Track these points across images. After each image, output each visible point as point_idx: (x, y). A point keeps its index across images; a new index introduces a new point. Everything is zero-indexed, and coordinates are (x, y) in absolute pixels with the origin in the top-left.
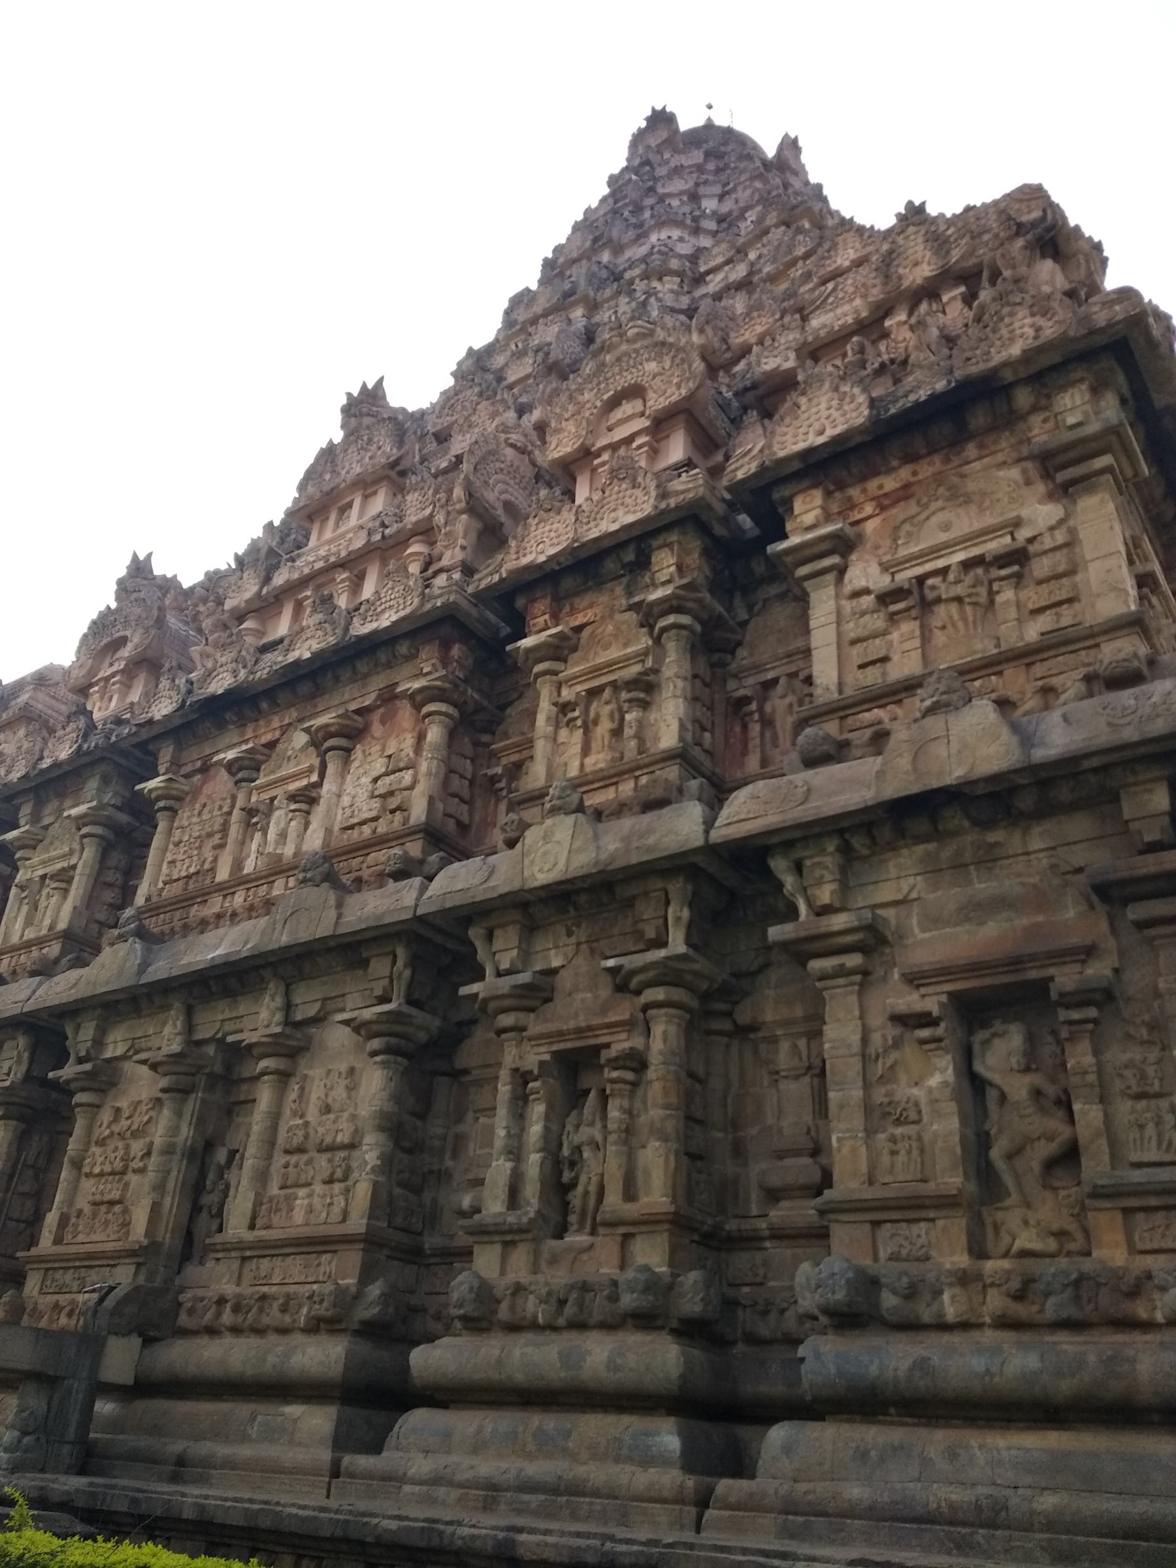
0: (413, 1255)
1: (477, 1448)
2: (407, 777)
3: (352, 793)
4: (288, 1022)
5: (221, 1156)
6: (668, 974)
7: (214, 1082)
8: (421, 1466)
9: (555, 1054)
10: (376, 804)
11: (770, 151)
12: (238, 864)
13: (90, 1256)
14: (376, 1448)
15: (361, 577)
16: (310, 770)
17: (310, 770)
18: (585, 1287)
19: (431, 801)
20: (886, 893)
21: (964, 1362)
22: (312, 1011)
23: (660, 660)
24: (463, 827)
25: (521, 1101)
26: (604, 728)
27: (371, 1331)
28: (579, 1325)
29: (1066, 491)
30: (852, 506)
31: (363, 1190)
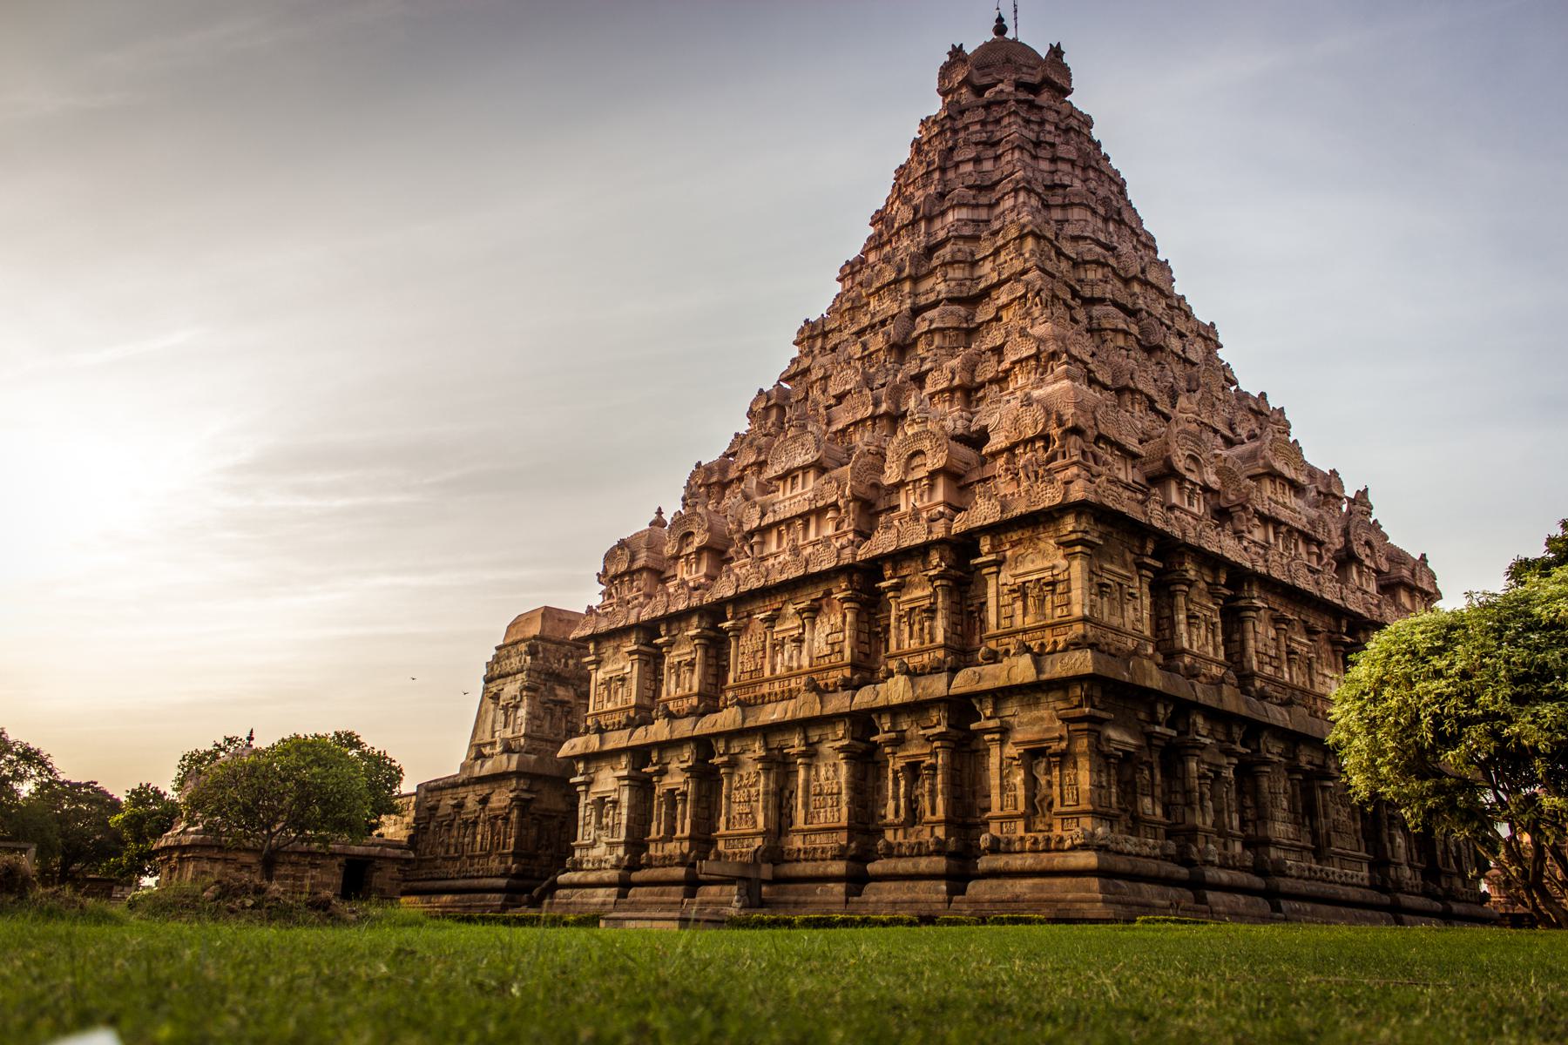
0: (867, 832)
1: (890, 892)
4: (807, 744)
5: (787, 793)
6: (940, 736)
7: (779, 766)
8: (873, 898)
11: (1043, 53)
12: (773, 669)
14: (859, 895)
18: (920, 844)
21: (1016, 862)
22: (816, 739)
24: (867, 656)
27: (852, 859)
28: (919, 855)
31: (845, 810)
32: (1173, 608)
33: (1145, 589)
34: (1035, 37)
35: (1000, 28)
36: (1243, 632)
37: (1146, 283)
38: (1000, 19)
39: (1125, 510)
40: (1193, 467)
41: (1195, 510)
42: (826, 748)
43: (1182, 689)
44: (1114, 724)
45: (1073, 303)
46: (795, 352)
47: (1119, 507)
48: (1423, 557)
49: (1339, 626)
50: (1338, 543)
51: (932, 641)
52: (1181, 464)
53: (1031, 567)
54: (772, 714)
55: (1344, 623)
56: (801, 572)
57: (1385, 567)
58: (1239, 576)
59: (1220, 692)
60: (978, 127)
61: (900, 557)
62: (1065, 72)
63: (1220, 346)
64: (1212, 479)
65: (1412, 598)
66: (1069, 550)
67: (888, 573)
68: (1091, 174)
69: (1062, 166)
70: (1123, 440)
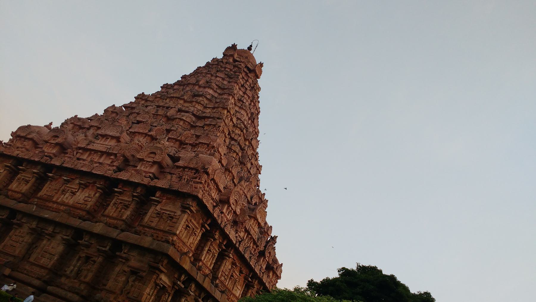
2: (90, 199)
3: (81, 196)
4: (53, 232)
5: (34, 246)
9: (86, 256)
10: (83, 201)
13: (7, 253)
15: (103, 155)
16: (76, 189)
17: (76, 189)
19: (91, 206)
20: (132, 254)
23: (131, 203)
24: (95, 211)
25: (78, 260)
26: (119, 209)
27: (44, 282)
28: (70, 291)
29: (183, 212)
30: (164, 196)
31: (52, 262)
32: (205, 245)
33: (200, 234)
34: (258, 56)
35: (250, 48)
36: (222, 263)
37: (250, 143)
38: (251, 46)
39: (208, 206)
40: (235, 204)
41: (228, 217)
42: (59, 237)
43: (193, 274)
44: (166, 274)
45: (227, 136)
46: (133, 100)
47: (207, 204)
48: (282, 264)
49: (249, 274)
50: (262, 248)
51: (121, 217)
52: (232, 201)
53: (169, 209)
54: (47, 215)
55: (251, 274)
56: (89, 171)
57: (271, 262)
58: (230, 244)
59: (204, 280)
60: (229, 70)
61: (128, 183)
62: (261, 72)
63: (260, 174)
64: (238, 211)
65: (273, 275)
66: (184, 210)
67: (120, 186)
68: (252, 104)
69: (246, 96)
70: (219, 184)
